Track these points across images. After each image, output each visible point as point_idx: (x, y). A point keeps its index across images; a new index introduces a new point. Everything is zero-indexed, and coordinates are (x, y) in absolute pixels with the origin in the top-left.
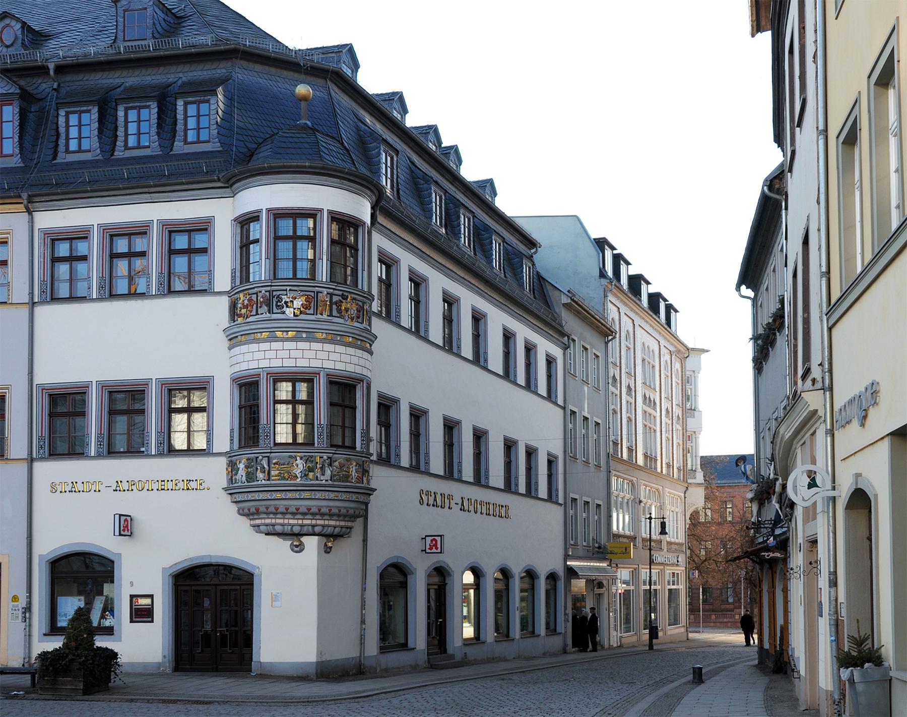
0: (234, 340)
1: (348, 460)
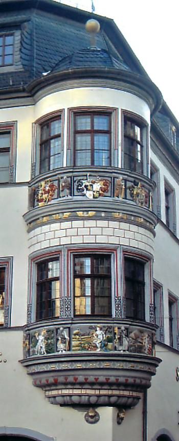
1: (141, 332)
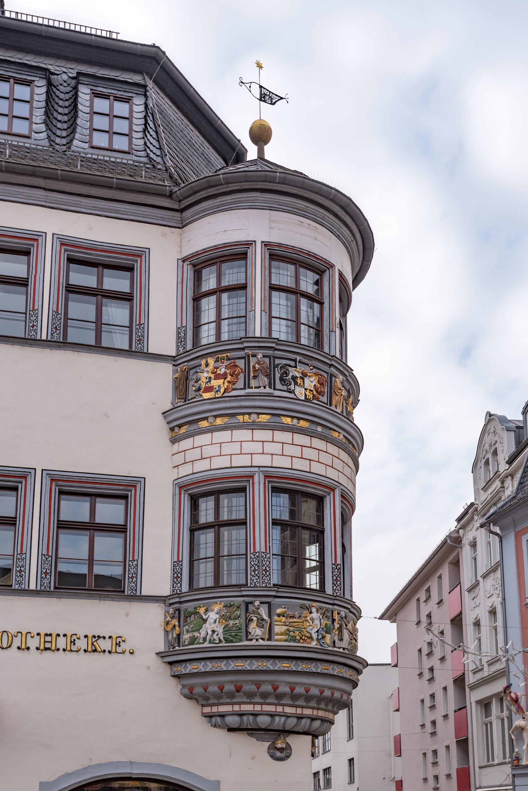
0: (180, 426)
